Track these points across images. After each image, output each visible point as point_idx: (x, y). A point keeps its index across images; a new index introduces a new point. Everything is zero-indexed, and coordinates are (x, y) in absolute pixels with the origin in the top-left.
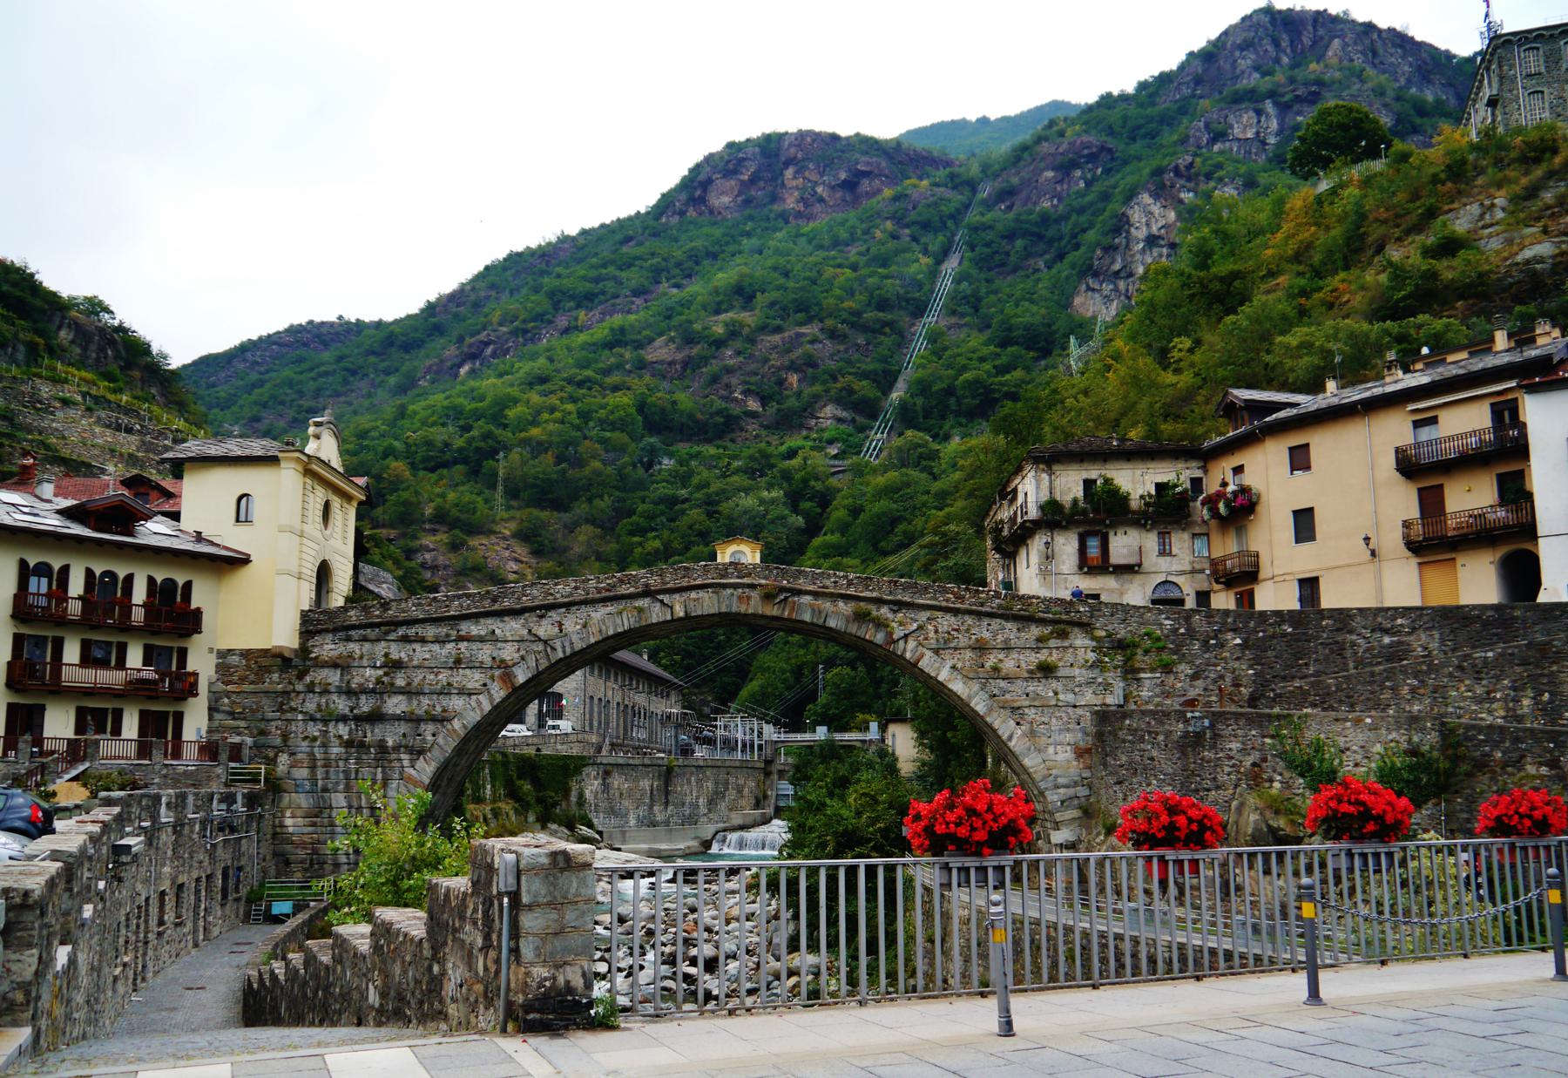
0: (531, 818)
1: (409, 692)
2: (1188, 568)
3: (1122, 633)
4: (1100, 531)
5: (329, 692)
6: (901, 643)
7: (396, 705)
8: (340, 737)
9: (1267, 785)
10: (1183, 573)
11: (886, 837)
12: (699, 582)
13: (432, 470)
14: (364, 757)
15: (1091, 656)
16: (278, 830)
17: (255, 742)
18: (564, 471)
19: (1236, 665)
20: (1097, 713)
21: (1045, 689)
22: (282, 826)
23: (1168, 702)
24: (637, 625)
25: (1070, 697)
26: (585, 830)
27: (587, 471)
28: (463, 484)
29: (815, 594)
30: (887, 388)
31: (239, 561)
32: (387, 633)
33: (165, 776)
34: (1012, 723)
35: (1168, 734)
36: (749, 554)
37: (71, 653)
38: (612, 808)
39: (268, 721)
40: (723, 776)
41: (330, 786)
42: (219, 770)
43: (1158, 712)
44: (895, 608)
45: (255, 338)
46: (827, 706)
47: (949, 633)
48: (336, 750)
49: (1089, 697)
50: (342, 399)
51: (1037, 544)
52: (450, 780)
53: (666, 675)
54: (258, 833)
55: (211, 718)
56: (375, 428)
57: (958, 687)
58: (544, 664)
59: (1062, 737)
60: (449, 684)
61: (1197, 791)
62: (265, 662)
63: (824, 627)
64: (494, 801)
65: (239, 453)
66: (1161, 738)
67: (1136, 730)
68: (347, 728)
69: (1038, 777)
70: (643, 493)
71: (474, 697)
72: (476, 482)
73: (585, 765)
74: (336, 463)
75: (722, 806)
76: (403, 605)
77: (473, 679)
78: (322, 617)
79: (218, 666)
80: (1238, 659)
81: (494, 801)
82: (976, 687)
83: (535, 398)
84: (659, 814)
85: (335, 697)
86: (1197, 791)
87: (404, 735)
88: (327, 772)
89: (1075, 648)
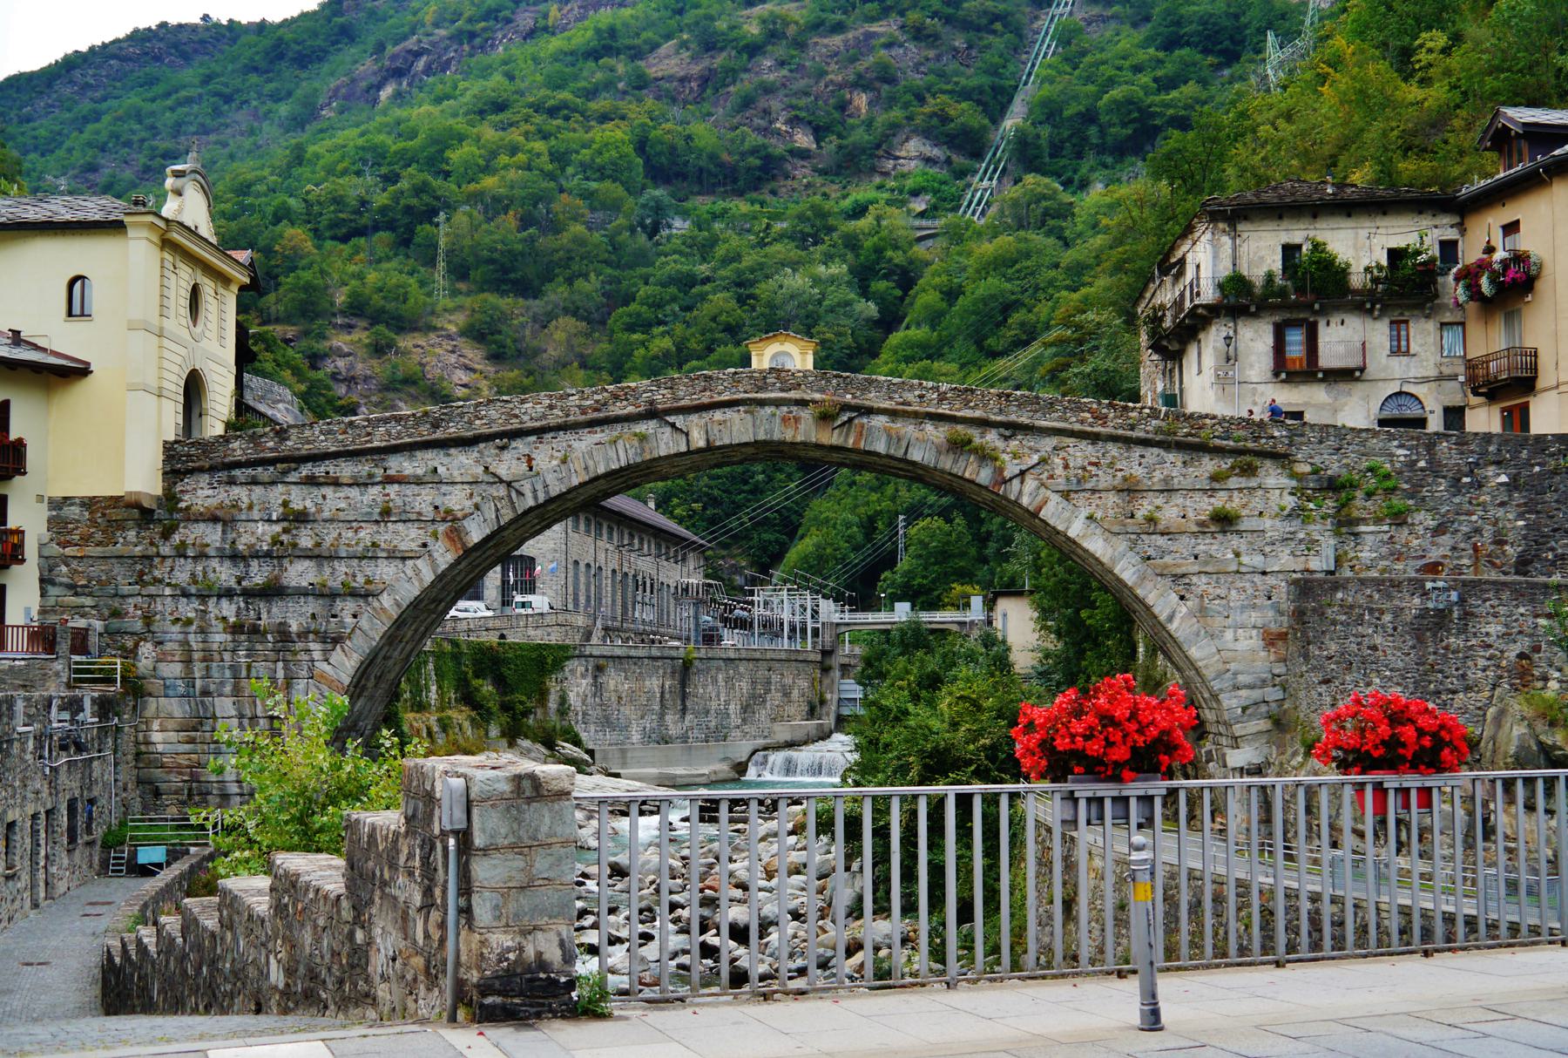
0: (494, 731)
1: (317, 556)
2: (1433, 373)
3: (1334, 468)
4: (1305, 320)
5: (207, 557)
6: (1016, 482)
7: (299, 574)
8: (224, 618)
9: (1539, 684)
10: (1426, 380)
11: (992, 758)
12: (725, 397)
13: (345, 239)
14: (259, 646)
15: (1290, 502)
16: (143, 748)
17: (106, 627)
18: (532, 239)
19: (1500, 513)
20: (1295, 582)
21: (1221, 548)
22: (148, 743)
23: (1399, 566)
24: (639, 460)
25: (1257, 561)
26: (569, 749)
27: (565, 239)
28: (389, 259)
29: (893, 414)
30: (997, 115)
31: (73, 372)
32: (285, 473)
34: (1174, 597)
35: (1398, 612)
36: (797, 355)
38: (607, 718)
39: (123, 597)
40: (762, 673)
41: (212, 687)
42: (58, 666)
43: (1383, 581)
44: (1007, 433)
45: (84, 48)
46: (909, 574)
47: (1084, 469)
48: (219, 638)
49: (1284, 560)
50: (213, 137)
51: (1213, 339)
52: (379, 679)
53: (681, 530)
54: (115, 752)
55: (43, 594)
56: (261, 179)
57: (1096, 545)
58: (507, 516)
59: (1245, 616)
60: (374, 544)
61: (1438, 693)
62: (115, 514)
63: (904, 460)
64: (442, 709)
65: (68, 217)
66: (1387, 618)
67: (1351, 607)
68: (234, 607)
69: (1209, 674)
70: (644, 270)
71: (410, 563)
72: (407, 257)
73: (568, 658)
74: (206, 230)
75: (762, 715)
76: (307, 433)
77: (408, 537)
78: (193, 451)
79: (49, 521)
80: (1502, 504)
81: (442, 709)
82: (1122, 545)
83: (489, 133)
84: (673, 725)
85: (215, 563)
86: (1438, 693)
87: (313, 616)
88: (208, 669)
89: (1266, 490)
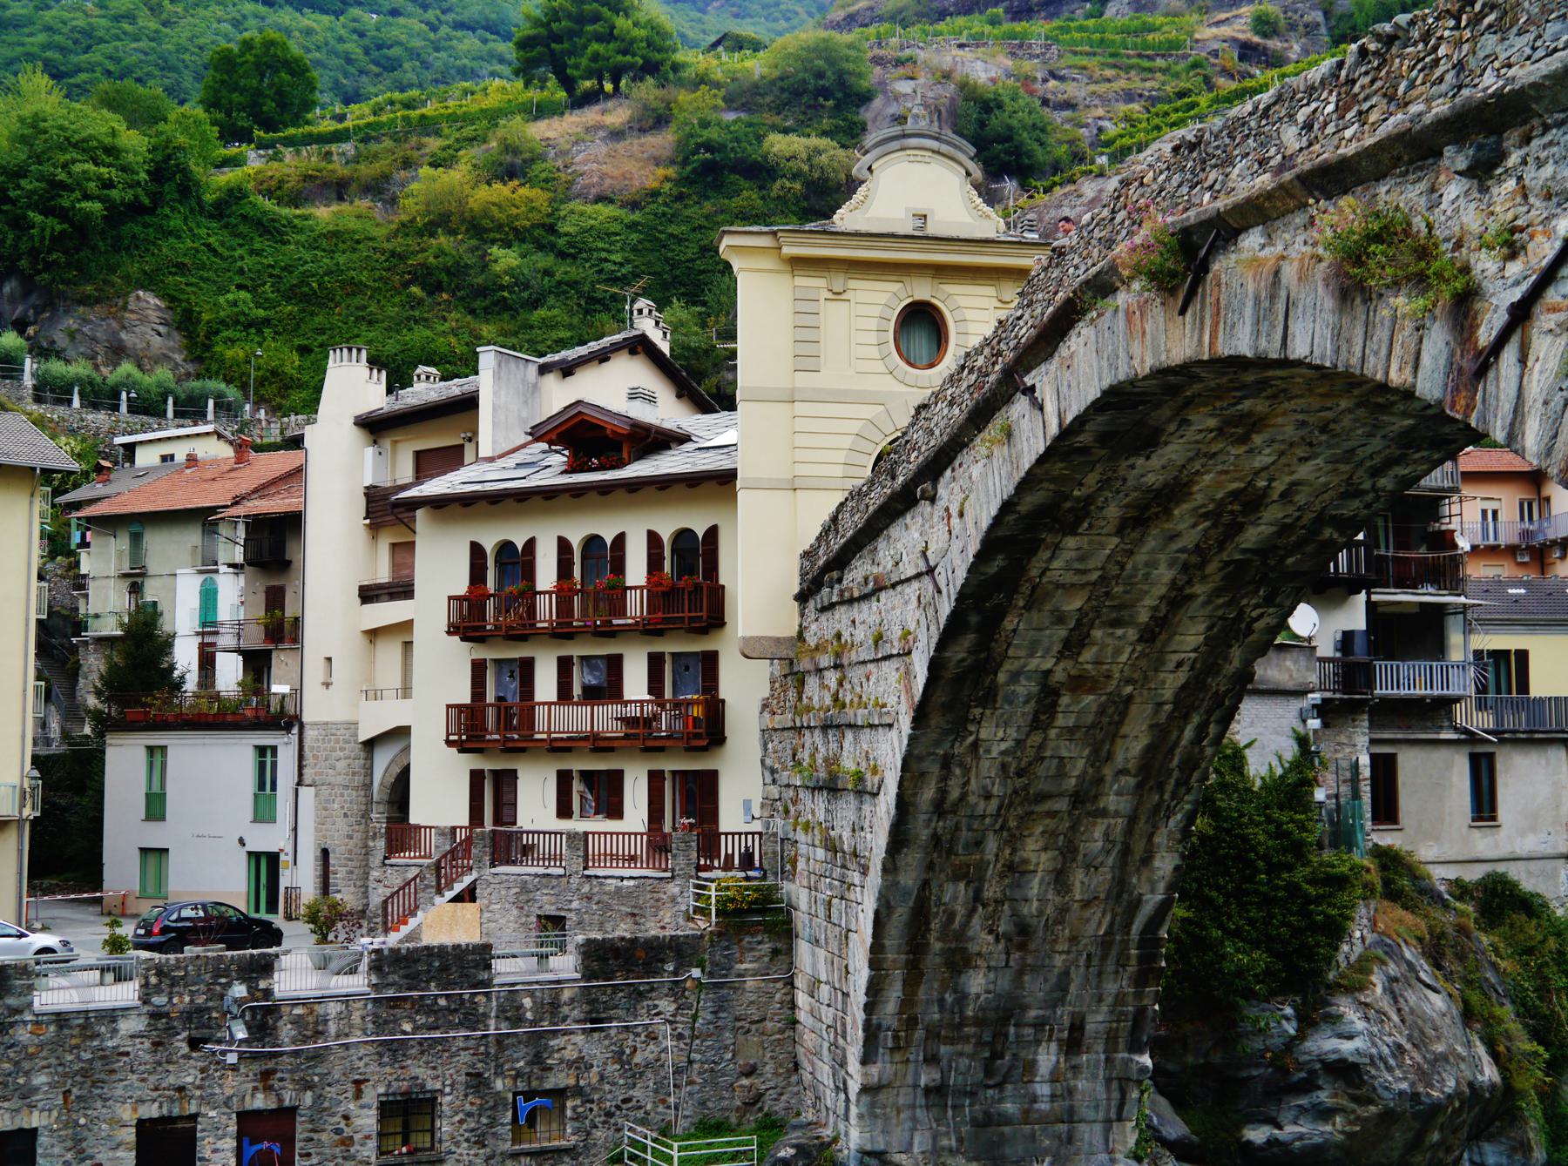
42: (674, 889)
52: (1021, 936)
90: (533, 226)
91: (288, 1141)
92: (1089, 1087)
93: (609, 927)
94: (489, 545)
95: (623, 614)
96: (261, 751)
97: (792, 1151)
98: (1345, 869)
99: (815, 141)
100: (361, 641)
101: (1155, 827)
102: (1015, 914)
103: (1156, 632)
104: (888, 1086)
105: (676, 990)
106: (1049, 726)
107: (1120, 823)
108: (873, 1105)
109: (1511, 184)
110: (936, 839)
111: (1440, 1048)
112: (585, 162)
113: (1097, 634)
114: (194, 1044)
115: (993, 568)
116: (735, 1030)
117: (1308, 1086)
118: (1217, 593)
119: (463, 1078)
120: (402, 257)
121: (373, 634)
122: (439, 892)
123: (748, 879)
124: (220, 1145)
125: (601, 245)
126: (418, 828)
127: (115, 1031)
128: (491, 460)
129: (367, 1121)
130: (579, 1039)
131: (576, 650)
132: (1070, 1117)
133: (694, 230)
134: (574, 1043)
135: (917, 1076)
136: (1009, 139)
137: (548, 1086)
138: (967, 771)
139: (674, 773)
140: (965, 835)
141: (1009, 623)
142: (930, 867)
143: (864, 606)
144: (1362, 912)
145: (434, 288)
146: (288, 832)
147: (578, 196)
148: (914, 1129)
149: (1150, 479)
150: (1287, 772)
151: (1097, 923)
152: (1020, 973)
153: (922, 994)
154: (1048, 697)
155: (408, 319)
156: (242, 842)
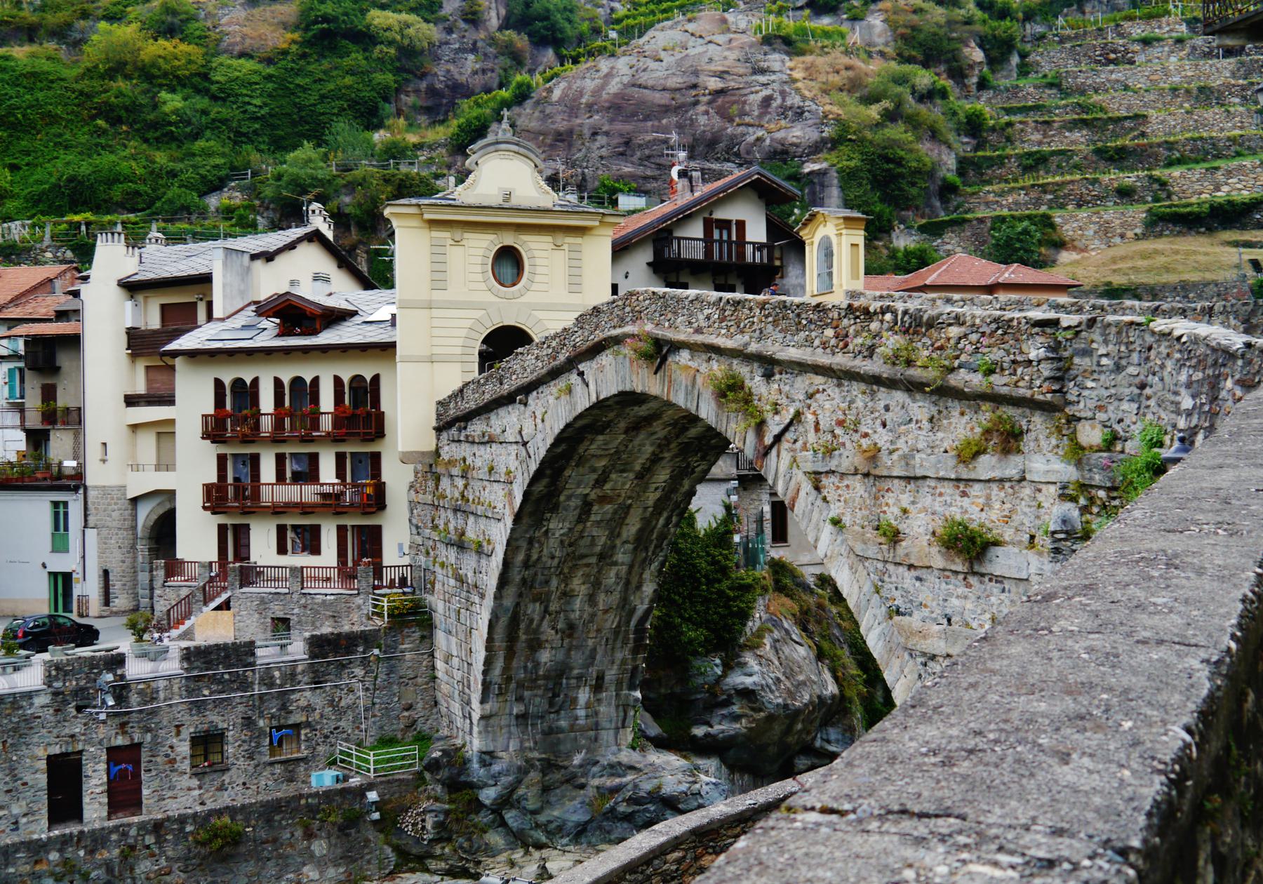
33: (305, 607)
37: (268, 471)
42: (359, 601)
90: (191, 74)
91: (137, 763)
92: (607, 710)
93: (318, 624)
94: (227, 381)
95: (318, 429)
96: (56, 504)
97: (440, 753)
98: (749, 581)
99: (404, 17)
100: (126, 431)
101: (643, 570)
102: (567, 618)
103: (644, 475)
104: (496, 715)
105: (365, 662)
106: (587, 520)
107: (624, 569)
108: (486, 726)
109: (776, 386)
110: (524, 581)
111: (801, 678)
112: (229, 24)
113: (613, 476)
114: (79, 709)
115: (559, 450)
116: (400, 684)
117: (727, 703)
118: (676, 456)
119: (240, 721)
120: (89, 96)
121: (135, 427)
122: (206, 603)
123: (404, 593)
124: (97, 767)
125: (245, 92)
126: (182, 562)
127: (32, 704)
128: (222, 320)
129: (184, 748)
130: (308, 694)
131: (287, 450)
132: (596, 727)
133: (315, 82)
134: (305, 696)
135: (512, 709)
136: (547, 18)
137: (290, 722)
138: (541, 545)
139: (353, 527)
140: (540, 578)
141: (567, 473)
142: (520, 595)
143: (482, 448)
144: (760, 603)
145: (115, 121)
146: (78, 558)
147: (225, 51)
148: (509, 738)
149: (641, 413)
150: (719, 525)
151: (612, 621)
152: (569, 650)
153: (515, 664)
154: (586, 507)
155: (97, 145)
156: (44, 566)
